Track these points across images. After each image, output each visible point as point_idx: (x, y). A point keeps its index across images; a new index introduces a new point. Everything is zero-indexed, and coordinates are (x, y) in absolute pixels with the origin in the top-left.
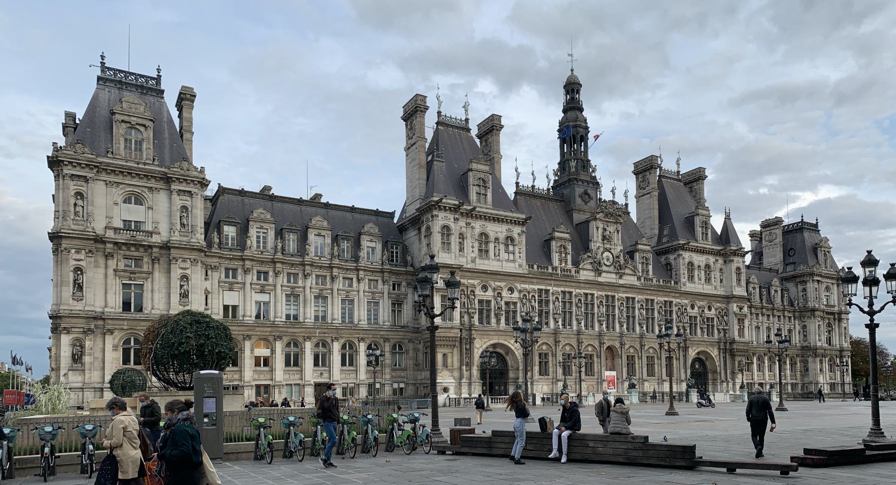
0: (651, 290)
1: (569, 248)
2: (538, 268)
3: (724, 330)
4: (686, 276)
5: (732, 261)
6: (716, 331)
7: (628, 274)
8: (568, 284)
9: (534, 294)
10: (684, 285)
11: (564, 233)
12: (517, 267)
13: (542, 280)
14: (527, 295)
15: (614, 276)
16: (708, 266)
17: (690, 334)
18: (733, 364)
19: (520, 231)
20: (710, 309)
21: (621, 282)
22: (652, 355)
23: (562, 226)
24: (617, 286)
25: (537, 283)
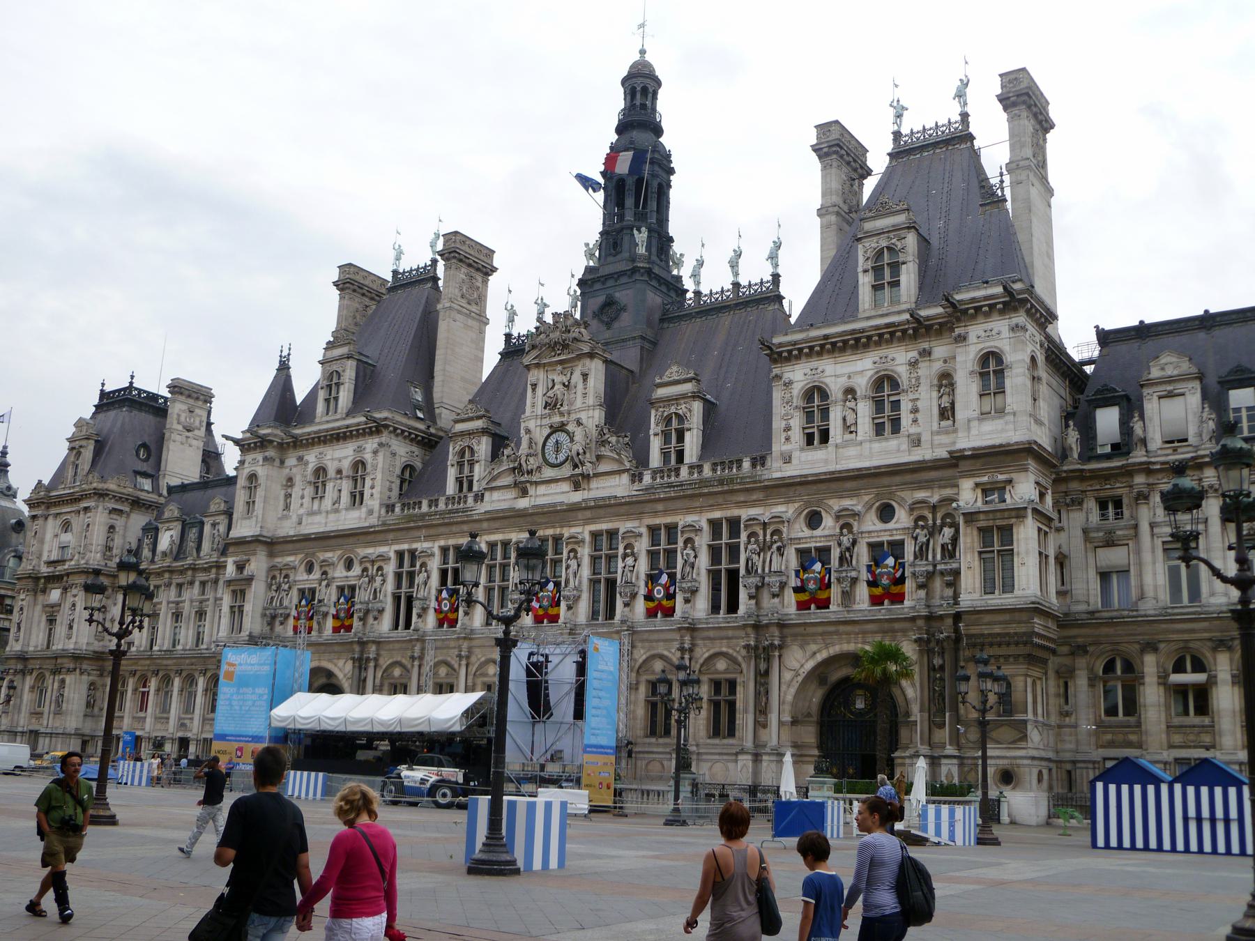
0: (660, 500)
1: (483, 447)
2: (403, 510)
7: (597, 475)
8: (454, 529)
10: (787, 459)
11: (470, 419)
12: (363, 516)
13: (404, 532)
14: (370, 568)
15: (565, 487)
16: (885, 382)
19: (375, 445)
20: (886, 513)
21: (577, 497)
24: (565, 511)
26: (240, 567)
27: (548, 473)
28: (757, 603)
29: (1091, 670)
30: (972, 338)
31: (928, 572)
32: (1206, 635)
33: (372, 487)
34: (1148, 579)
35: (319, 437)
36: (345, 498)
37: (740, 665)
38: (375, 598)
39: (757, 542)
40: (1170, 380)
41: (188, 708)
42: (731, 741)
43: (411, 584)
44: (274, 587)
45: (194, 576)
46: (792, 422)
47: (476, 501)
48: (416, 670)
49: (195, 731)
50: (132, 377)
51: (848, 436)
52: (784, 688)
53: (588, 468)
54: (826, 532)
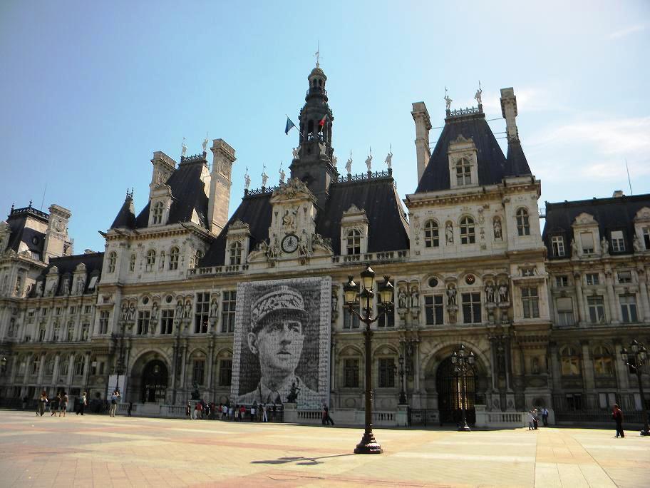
0: (350, 270)
1: (246, 243)
2: (201, 272)
3: (501, 308)
4: (422, 242)
5: (508, 201)
6: (484, 313)
7: (313, 258)
9: (190, 299)
10: (418, 253)
12: (178, 275)
15: (296, 263)
16: (467, 221)
17: (429, 321)
18: (523, 361)
21: (303, 268)
22: (354, 357)
23: (238, 222)
25: (198, 287)
26: (106, 299)
27: (285, 256)
28: (405, 321)
29: (558, 353)
30: (513, 201)
31: (494, 309)
32: (611, 337)
33: (183, 261)
34: (582, 313)
35: (151, 235)
36: (167, 265)
37: (396, 351)
38: (186, 316)
39: (404, 292)
40: (586, 226)
41: (63, 372)
42: (392, 388)
43: (207, 310)
44: (125, 310)
45: (67, 303)
46: (419, 236)
47: (244, 269)
48: (211, 353)
49: (68, 383)
50: (31, 203)
51: (449, 243)
52: (421, 362)
53: (309, 255)
54: (440, 288)
